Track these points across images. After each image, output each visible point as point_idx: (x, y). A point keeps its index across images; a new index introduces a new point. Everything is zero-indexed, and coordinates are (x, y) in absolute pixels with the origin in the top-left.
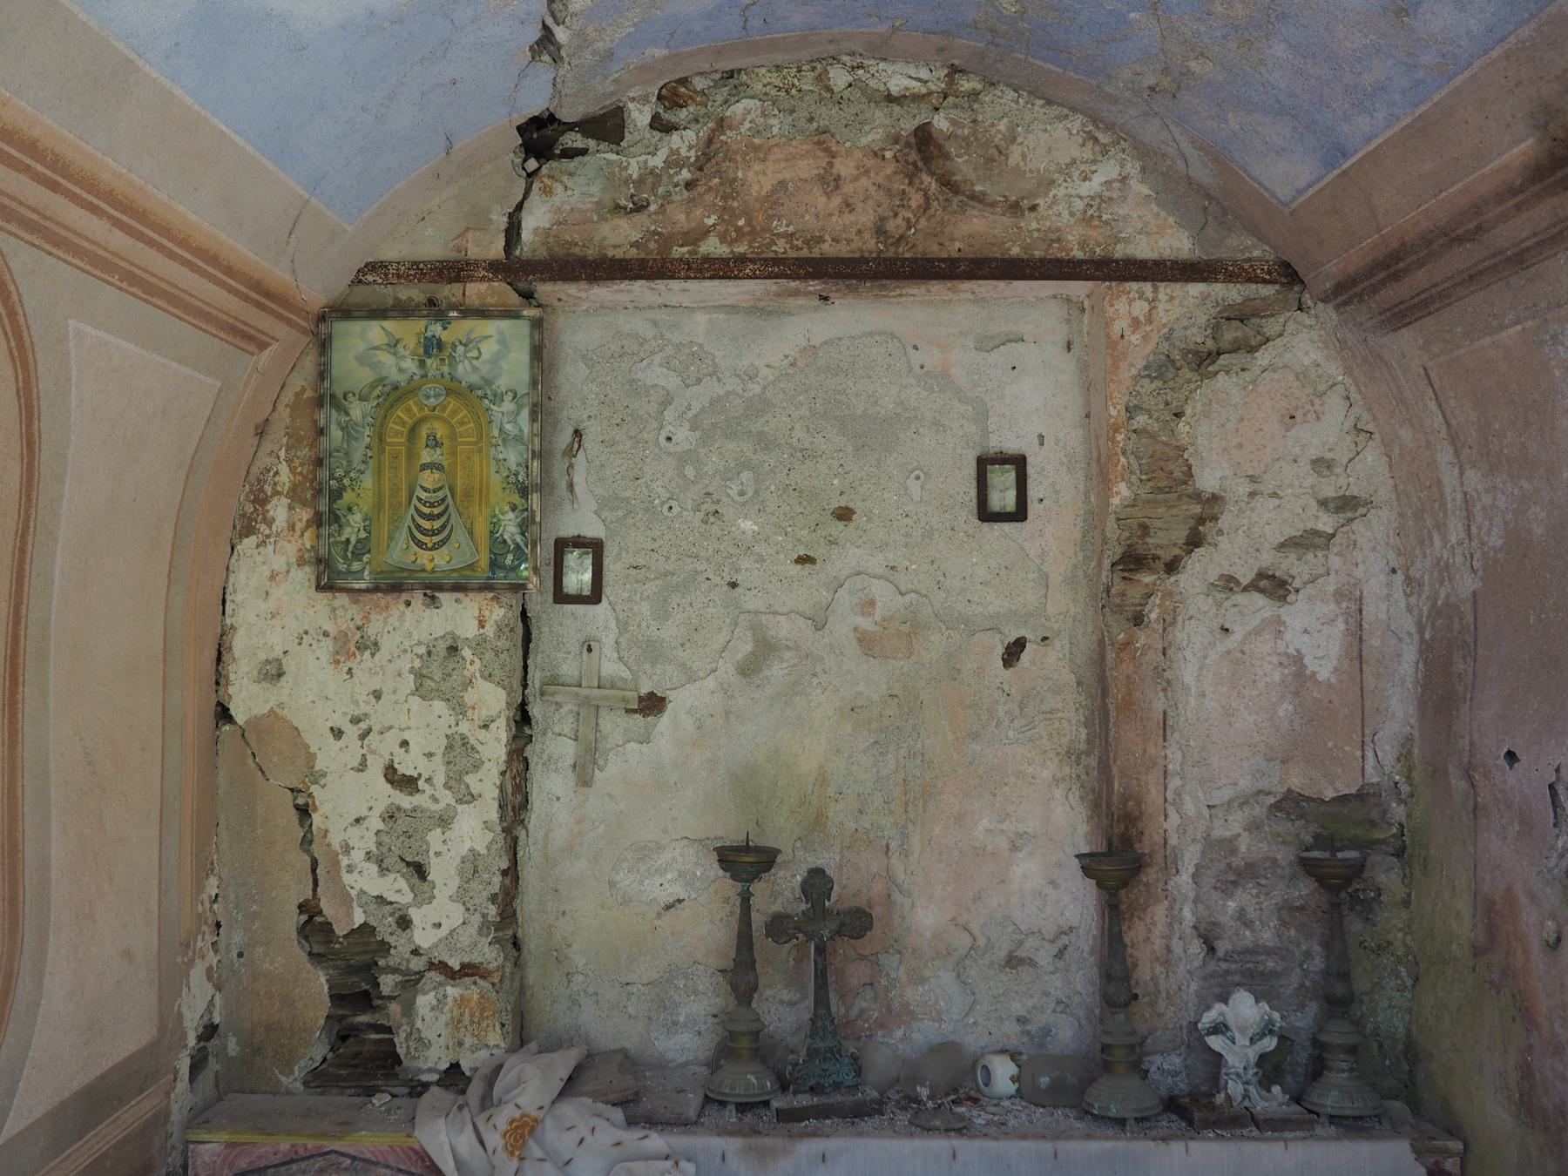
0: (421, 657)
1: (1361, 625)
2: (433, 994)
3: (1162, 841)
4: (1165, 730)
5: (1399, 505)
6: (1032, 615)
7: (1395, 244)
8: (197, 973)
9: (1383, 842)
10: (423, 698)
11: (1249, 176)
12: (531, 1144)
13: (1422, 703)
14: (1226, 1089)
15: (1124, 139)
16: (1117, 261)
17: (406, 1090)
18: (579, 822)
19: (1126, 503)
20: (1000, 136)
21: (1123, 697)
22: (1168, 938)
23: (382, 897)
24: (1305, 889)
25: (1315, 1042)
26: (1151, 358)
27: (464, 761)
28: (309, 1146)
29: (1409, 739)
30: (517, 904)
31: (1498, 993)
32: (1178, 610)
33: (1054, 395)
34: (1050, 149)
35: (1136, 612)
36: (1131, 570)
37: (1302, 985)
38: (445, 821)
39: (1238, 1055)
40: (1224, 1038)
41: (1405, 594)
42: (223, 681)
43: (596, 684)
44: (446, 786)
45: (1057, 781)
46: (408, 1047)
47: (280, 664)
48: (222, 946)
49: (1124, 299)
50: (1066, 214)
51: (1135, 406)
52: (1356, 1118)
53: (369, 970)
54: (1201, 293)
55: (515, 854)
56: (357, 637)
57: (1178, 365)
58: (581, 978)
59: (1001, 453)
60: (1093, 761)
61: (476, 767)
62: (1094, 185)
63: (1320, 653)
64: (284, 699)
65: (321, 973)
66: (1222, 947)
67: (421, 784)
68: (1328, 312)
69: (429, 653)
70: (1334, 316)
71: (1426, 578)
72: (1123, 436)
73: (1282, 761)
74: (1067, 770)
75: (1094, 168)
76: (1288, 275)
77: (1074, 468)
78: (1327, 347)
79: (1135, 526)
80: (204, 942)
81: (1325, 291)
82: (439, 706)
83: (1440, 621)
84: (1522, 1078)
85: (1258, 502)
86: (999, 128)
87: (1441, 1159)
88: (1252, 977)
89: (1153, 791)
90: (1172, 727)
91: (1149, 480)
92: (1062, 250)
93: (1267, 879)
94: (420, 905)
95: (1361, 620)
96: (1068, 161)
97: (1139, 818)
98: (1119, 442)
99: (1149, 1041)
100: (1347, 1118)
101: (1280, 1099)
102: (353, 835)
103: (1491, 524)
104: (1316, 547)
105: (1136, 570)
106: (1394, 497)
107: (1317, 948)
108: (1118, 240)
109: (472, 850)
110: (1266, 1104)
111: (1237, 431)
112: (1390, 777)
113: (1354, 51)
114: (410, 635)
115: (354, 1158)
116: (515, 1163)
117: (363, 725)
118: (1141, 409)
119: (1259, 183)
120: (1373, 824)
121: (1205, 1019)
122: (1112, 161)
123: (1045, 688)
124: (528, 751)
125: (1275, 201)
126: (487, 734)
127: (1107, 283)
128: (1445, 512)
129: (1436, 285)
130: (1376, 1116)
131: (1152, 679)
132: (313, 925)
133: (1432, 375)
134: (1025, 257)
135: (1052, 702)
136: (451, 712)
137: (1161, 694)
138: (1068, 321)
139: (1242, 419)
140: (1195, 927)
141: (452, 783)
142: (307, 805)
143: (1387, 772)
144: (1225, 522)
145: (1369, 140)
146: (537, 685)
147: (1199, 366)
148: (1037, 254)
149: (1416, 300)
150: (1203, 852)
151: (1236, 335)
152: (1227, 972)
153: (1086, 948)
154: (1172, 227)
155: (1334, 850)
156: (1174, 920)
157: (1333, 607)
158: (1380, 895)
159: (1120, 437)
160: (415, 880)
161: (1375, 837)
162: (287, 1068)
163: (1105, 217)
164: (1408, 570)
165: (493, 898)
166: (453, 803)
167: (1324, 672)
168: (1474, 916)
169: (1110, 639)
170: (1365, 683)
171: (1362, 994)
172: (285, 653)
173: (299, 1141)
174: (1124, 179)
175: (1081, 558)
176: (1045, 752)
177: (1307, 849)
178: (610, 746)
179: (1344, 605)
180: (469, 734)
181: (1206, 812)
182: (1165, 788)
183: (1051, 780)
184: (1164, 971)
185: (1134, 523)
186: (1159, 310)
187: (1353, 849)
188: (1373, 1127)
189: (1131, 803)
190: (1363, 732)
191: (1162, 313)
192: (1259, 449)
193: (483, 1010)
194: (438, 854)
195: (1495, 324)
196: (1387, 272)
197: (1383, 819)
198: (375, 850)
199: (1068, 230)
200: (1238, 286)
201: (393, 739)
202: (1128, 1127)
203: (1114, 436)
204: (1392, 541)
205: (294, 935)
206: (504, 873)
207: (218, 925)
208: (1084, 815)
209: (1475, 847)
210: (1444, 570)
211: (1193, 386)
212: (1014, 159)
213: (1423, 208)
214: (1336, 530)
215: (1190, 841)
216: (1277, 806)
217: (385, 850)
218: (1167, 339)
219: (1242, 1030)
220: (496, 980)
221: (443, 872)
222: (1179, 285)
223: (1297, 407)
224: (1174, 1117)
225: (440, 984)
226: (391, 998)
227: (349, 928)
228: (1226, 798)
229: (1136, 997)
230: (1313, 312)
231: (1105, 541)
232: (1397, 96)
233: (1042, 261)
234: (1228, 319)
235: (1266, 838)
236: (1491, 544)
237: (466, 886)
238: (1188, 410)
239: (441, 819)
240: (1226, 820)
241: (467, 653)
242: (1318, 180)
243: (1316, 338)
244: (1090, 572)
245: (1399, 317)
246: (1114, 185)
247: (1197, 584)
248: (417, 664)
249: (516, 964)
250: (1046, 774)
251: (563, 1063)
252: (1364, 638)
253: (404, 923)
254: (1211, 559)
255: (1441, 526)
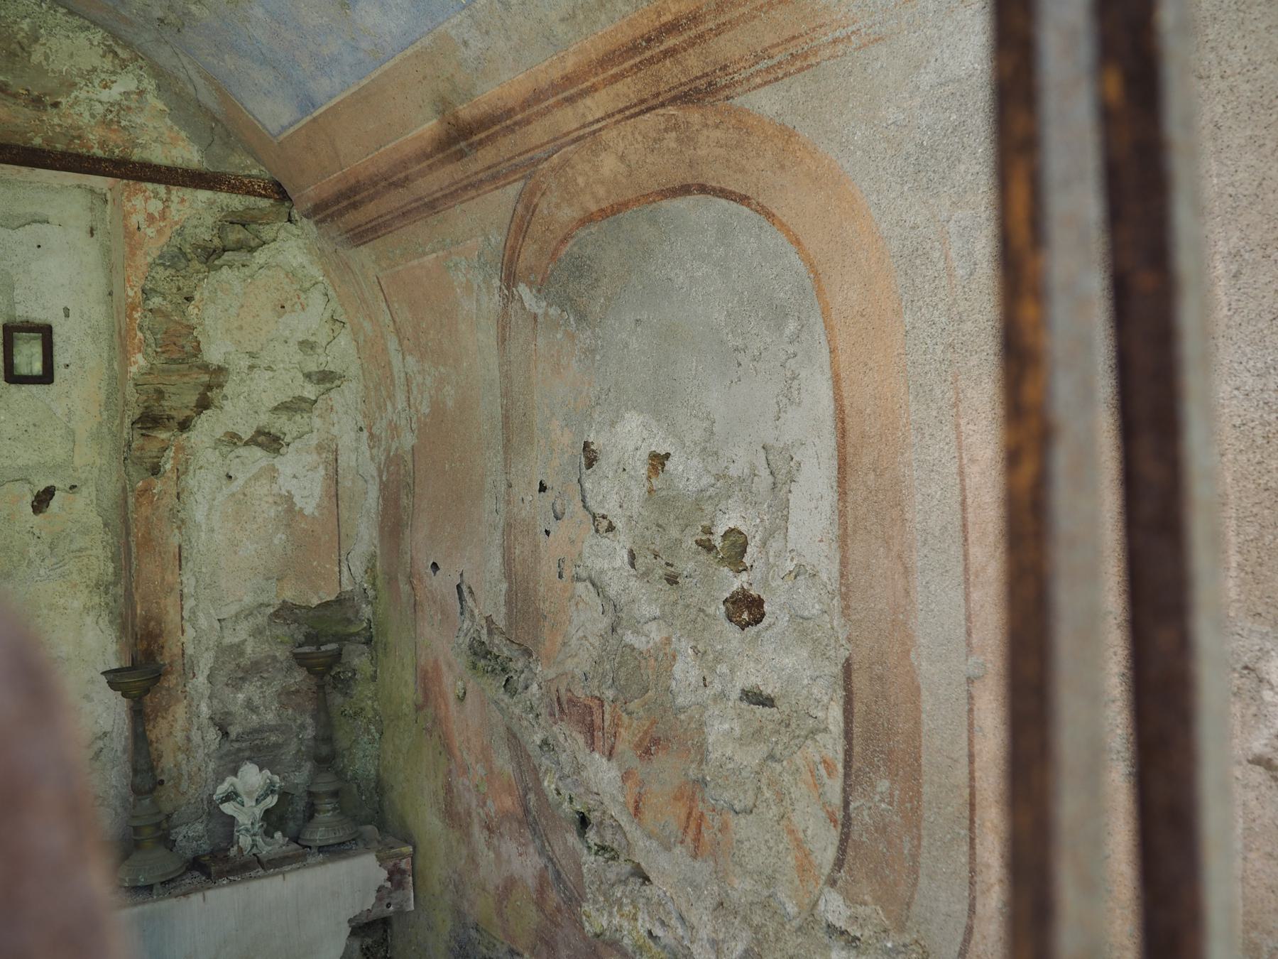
1: (337, 471)
3: (181, 652)
4: (180, 561)
5: (365, 379)
6: (60, 467)
7: (352, 181)
9: (358, 634)
11: (245, 108)
13: (382, 529)
14: (238, 843)
15: (141, 58)
16: (134, 163)
19: (143, 371)
20: (22, 34)
21: (143, 535)
22: (188, 730)
24: (299, 677)
25: (310, 794)
26: (165, 249)
29: (374, 556)
31: (431, 736)
32: (190, 461)
33: (78, 273)
34: (72, 54)
35: (154, 463)
36: (149, 428)
37: (299, 750)
39: (246, 814)
40: (234, 803)
41: (369, 446)
45: (87, 609)
49: (140, 196)
50: (87, 114)
51: (151, 289)
52: (339, 844)
54: (208, 199)
57: (189, 256)
59: (28, 322)
60: (120, 590)
62: (115, 93)
63: (306, 493)
66: (234, 731)
68: (309, 225)
70: (315, 230)
71: (383, 435)
72: (139, 314)
73: (277, 579)
74: (96, 599)
75: (113, 78)
76: (279, 192)
77: (98, 339)
78: (310, 253)
79: (151, 391)
81: (307, 210)
83: (392, 467)
84: (446, 794)
85: (256, 374)
86: (22, 26)
87: (398, 861)
88: (260, 751)
89: (172, 612)
90: (186, 558)
91: (163, 352)
92: (83, 147)
93: (269, 672)
95: (337, 467)
96: (90, 68)
97: (160, 635)
98: (136, 319)
99: (175, 816)
100: (332, 845)
101: (281, 842)
103: (422, 397)
104: (303, 410)
105: (153, 428)
106: (361, 373)
107: (309, 721)
108: (135, 145)
110: (270, 848)
111: (238, 315)
112: (360, 585)
113: (314, 27)
118: (156, 291)
119: (253, 116)
120: (349, 621)
121: (218, 792)
122: (131, 76)
123: (74, 530)
125: (266, 132)
127: (125, 181)
128: (394, 386)
129: (381, 216)
130: (353, 840)
131: (169, 519)
133: (382, 283)
134: (47, 148)
135: (80, 542)
137: (176, 531)
138: (92, 209)
139: (242, 306)
140: (211, 718)
143: (358, 582)
144: (228, 389)
145: (330, 98)
147: (207, 259)
148: (59, 147)
149: (369, 226)
150: (216, 657)
151: (238, 236)
152: (239, 750)
153: (120, 748)
154: (183, 140)
155: (319, 644)
156: (193, 714)
157: (315, 456)
158: (355, 674)
159: (137, 315)
161: (352, 631)
163: (123, 123)
164: (371, 429)
167: (310, 507)
168: (416, 682)
169: (132, 486)
170: (340, 515)
171: (343, 750)
174: (141, 93)
175: (105, 417)
176: (75, 585)
177: (300, 646)
179: (324, 455)
181: (217, 625)
182: (182, 608)
183: (82, 609)
184: (185, 757)
185: (151, 388)
186: (172, 209)
187: (335, 642)
188: (351, 849)
189: (152, 623)
190: (339, 553)
191: (174, 213)
192: (256, 331)
195: (420, 250)
196: (348, 202)
197: (356, 617)
199: (89, 129)
200: (240, 196)
202: (154, 891)
203: (131, 313)
204: (359, 406)
208: (113, 636)
209: (416, 633)
210: (394, 428)
211: (201, 276)
212: (37, 57)
213: (370, 156)
214: (318, 397)
215: (203, 649)
216: (276, 615)
218: (179, 235)
219: (249, 794)
222: (189, 190)
223: (287, 299)
224: (196, 874)
228: (233, 612)
229: (162, 782)
230: (299, 224)
231: (126, 404)
232: (347, 69)
233: (63, 154)
234: (232, 223)
235: (267, 641)
236: (422, 412)
238: (197, 296)
240: (234, 630)
242: (297, 121)
243: (302, 245)
244: (114, 429)
245: (360, 236)
246: (132, 96)
247: (205, 439)
250: (77, 604)
252: (339, 480)
254: (217, 420)
255: (391, 397)
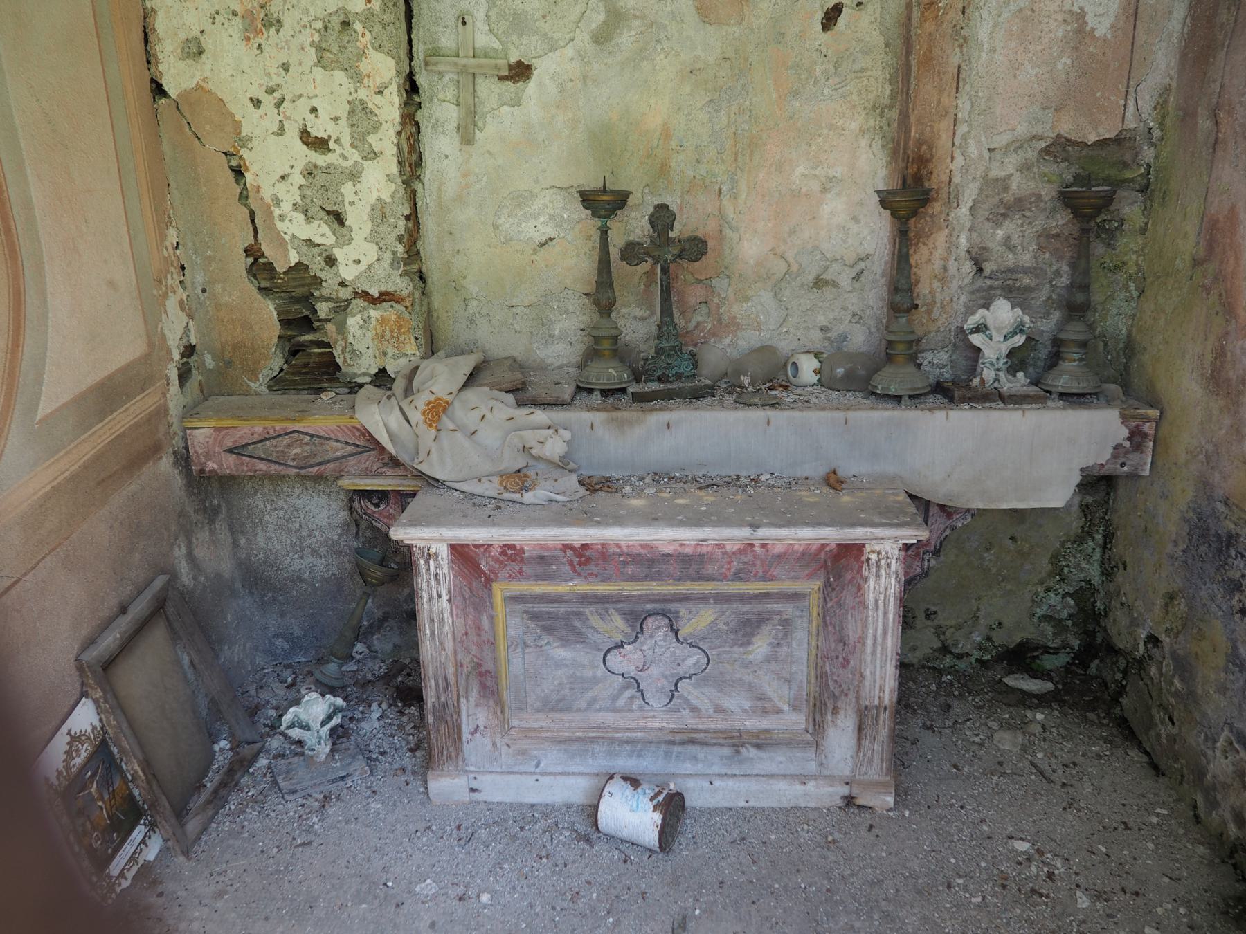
0: (319, 31)
2: (359, 316)
8: (172, 303)
9: (1132, 180)
10: (325, 68)
12: (444, 418)
13: (1183, 56)
17: (347, 390)
18: (466, 175)
22: (946, 259)
23: (310, 240)
24: (1062, 220)
27: (365, 123)
28: (277, 428)
29: (1167, 89)
30: (420, 245)
37: (1049, 298)
38: (354, 175)
39: (993, 349)
42: (152, 60)
43: (472, 55)
44: (352, 145)
45: (862, 132)
46: (345, 358)
47: (199, 43)
48: (188, 283)
53: (307, 300)
55: (415, 204)
56: (262, 15)
58: (475, 303)
60: (894, 114)
61: (376, 128)
63: (1101, 10)
64: (208, 74)
65: (269, 303)
66: (989, 267)
67: (332, 144)
69: (326, 28)
73: (1055, 110)
74: (872, 122)
80: (173, 279)
82: (339, 76)
84: (1216, 358)
89: (944, 136)
90: (965, 80)
94: (341, 246)
97: (929, 160)
99: (924, 341)
102: (281, 190)
107: (1065, 268)
109: (379, 199)
110: (1011, 385)
114: (307, 11)
115: (312, 436)
116: (433, 432)
117: (277, 95)
120: (1125, 165)
123: (857, 49)
124: (419, 116)
126: (382, 99)
131: (951, 36)
132: (258, 266)
135: (863, 62)
136: (350, 81)
137: (958, 50)
140: (968, 252)
141: (357, 143)
142: (240, 166)
143: (1144, 119)
146: (422, 57)
150: (981, 190)
152: (991, 288)
153: (879, 272)
156: (951, 245)
160: (336, 225)
161: (1126, 176)
162: (254, 374)
165: (400, 238)
166: (360, 160)
167: (1102, 27)
168: (1199, 234)
170: (1136, 38)
172: (202, 32)
173: (269, 424)
176: (854, 106)
178: (486, 109)
180: (366, 99)
181: (986, 154)
182: (954, 134)
189: (924, 147)
193: (400, 327)
194: (352, 203)
197: (1134, 160)
198: (300, 201)
201: (303, 106)
202: (903, 402)
205: (244, 273)
206: (407, 218)
207: (183, 268)
209: (1210, 177)
215: (970, 178)
216: (1046, 151)
217: (308, 201)
219: (998, 329)
220: (408, 304)
221: (357, 218)
224: (939, 396)
225: (364, 308)
226: (328, 321)
227: (287, 266)
228: (1004, 143)
229: (916, 306)
237: (377, 229)
239: (351, 174)
241: (358, 26)
248: (316, 38)
249: (423, 293)
250: (854, 126)
251: (466, 365)
253: (331, 261)
